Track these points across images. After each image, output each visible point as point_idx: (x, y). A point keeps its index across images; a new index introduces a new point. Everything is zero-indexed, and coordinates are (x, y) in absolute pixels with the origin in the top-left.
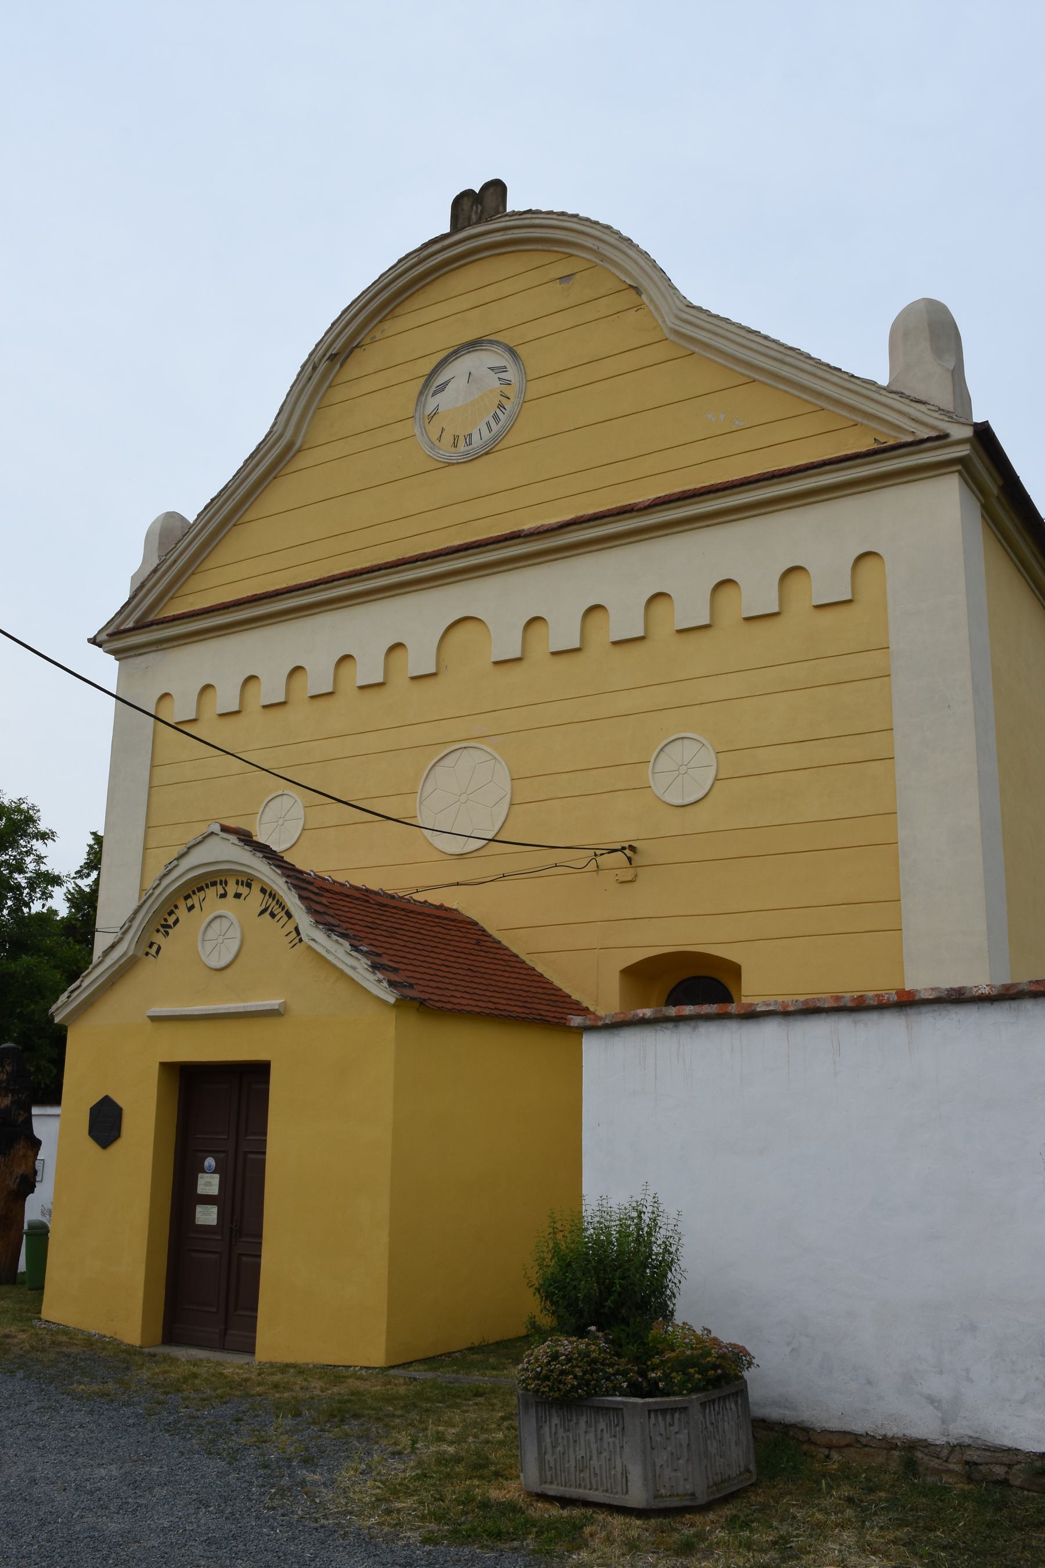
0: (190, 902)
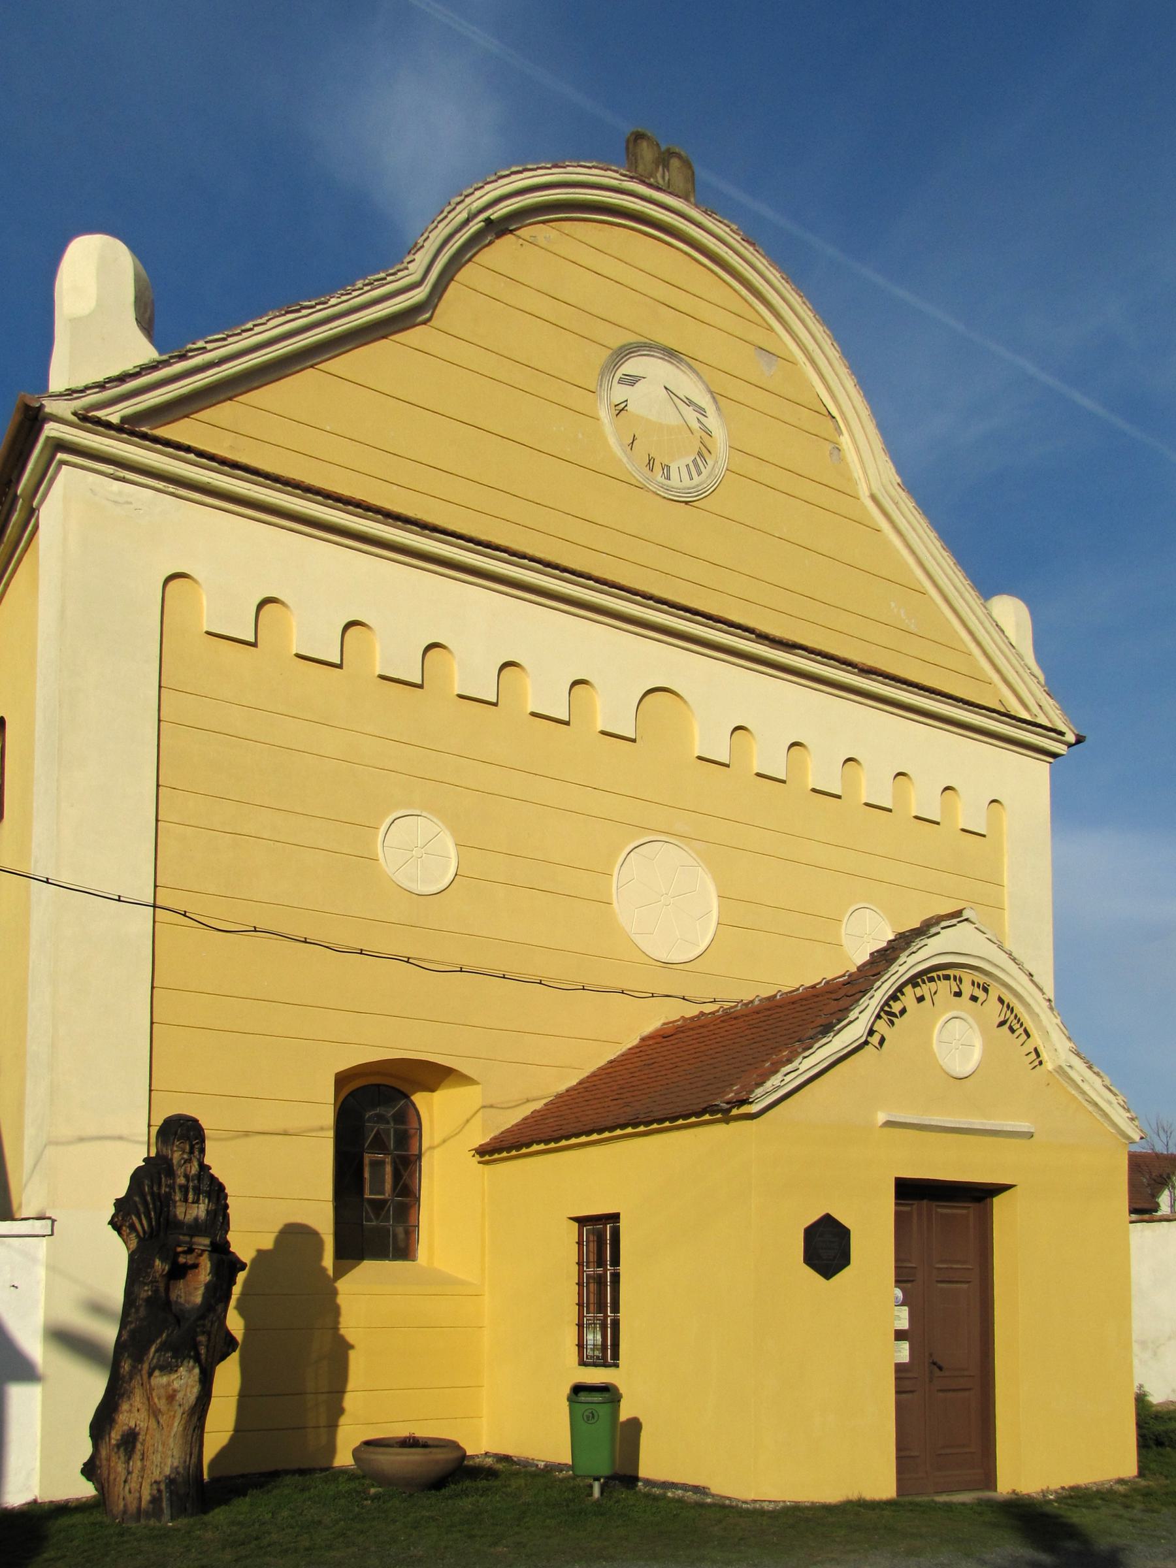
0: (919, 992)
